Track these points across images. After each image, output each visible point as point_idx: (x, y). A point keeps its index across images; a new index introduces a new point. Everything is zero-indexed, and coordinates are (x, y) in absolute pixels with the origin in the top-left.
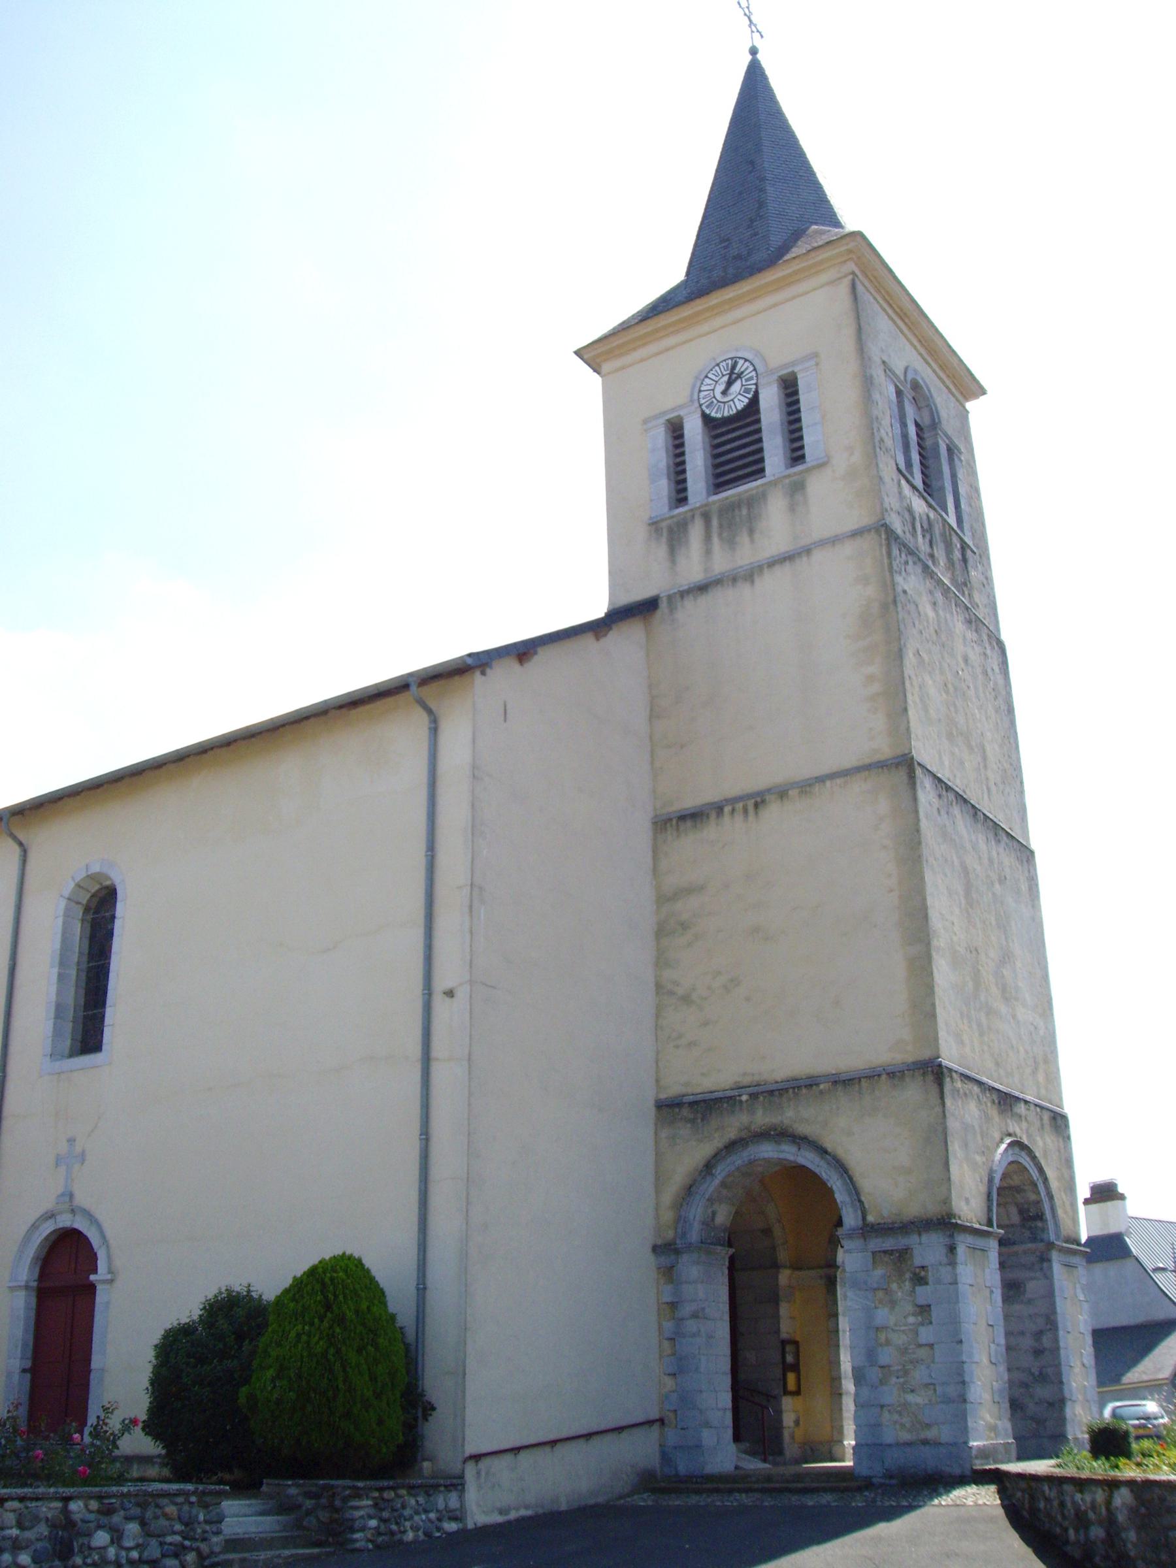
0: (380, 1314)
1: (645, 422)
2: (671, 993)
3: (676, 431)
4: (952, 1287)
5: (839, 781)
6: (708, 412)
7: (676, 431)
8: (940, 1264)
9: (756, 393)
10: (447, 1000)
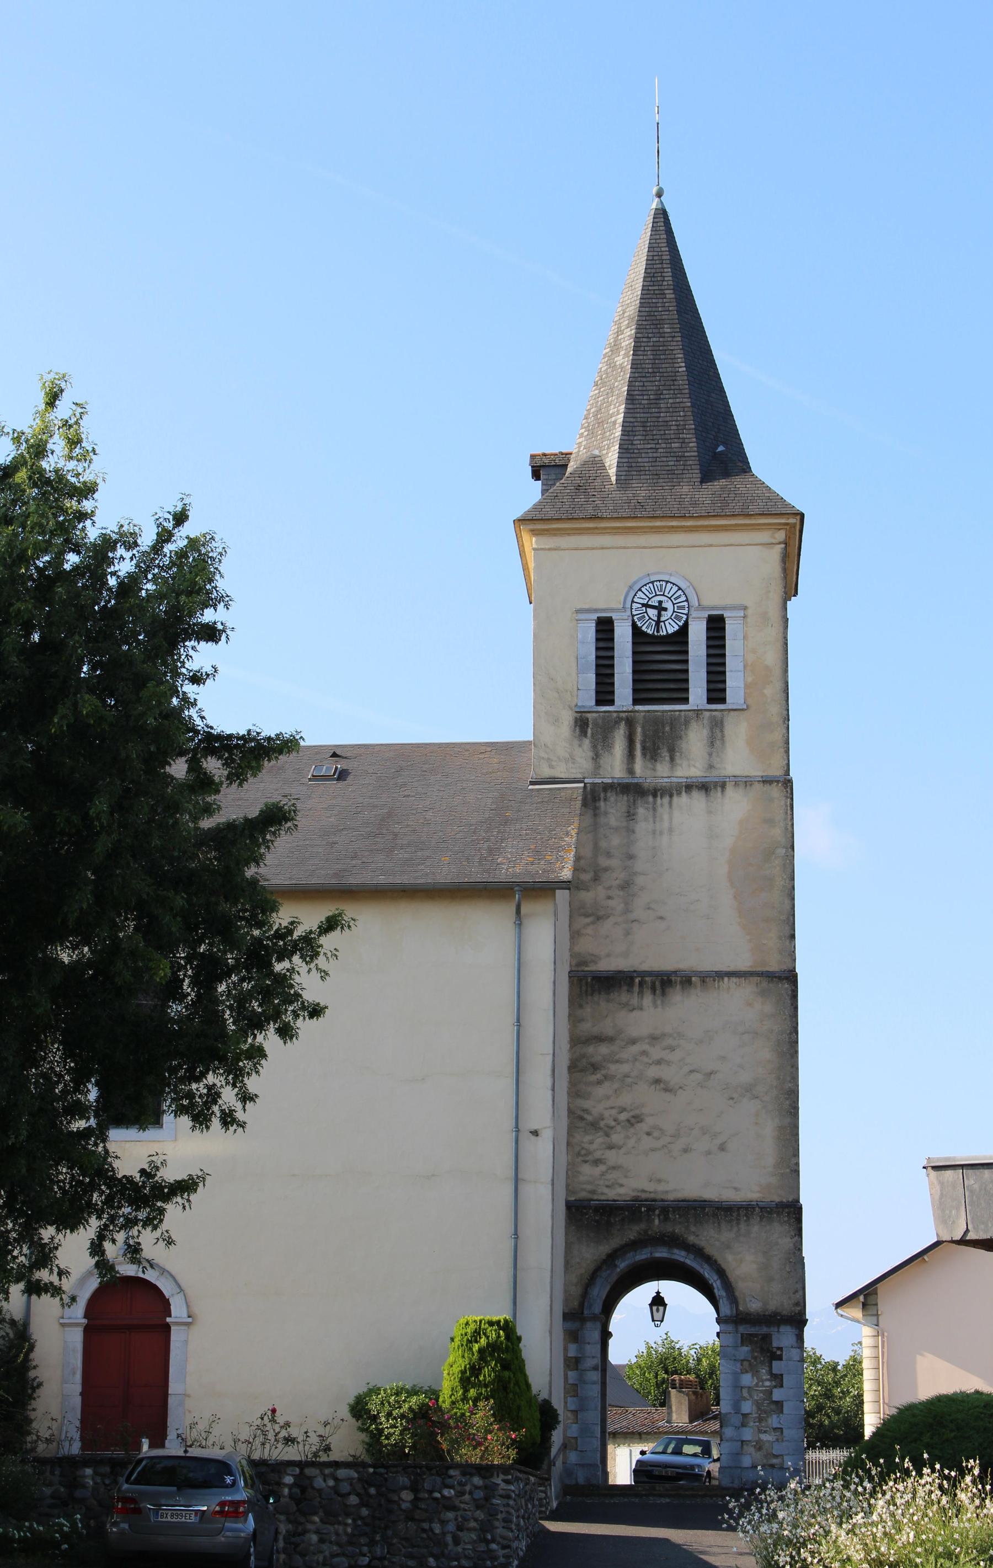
0: (509, 1377)
1: (579, 611)
2: (582, 1118)
3: (605, 628)
4: (799, 1363)
5: (734, 980)
6: (639, 624)
7: (605, 628)
8: (792, 1347)
9: (686, 624)
10: (533, 1138)
